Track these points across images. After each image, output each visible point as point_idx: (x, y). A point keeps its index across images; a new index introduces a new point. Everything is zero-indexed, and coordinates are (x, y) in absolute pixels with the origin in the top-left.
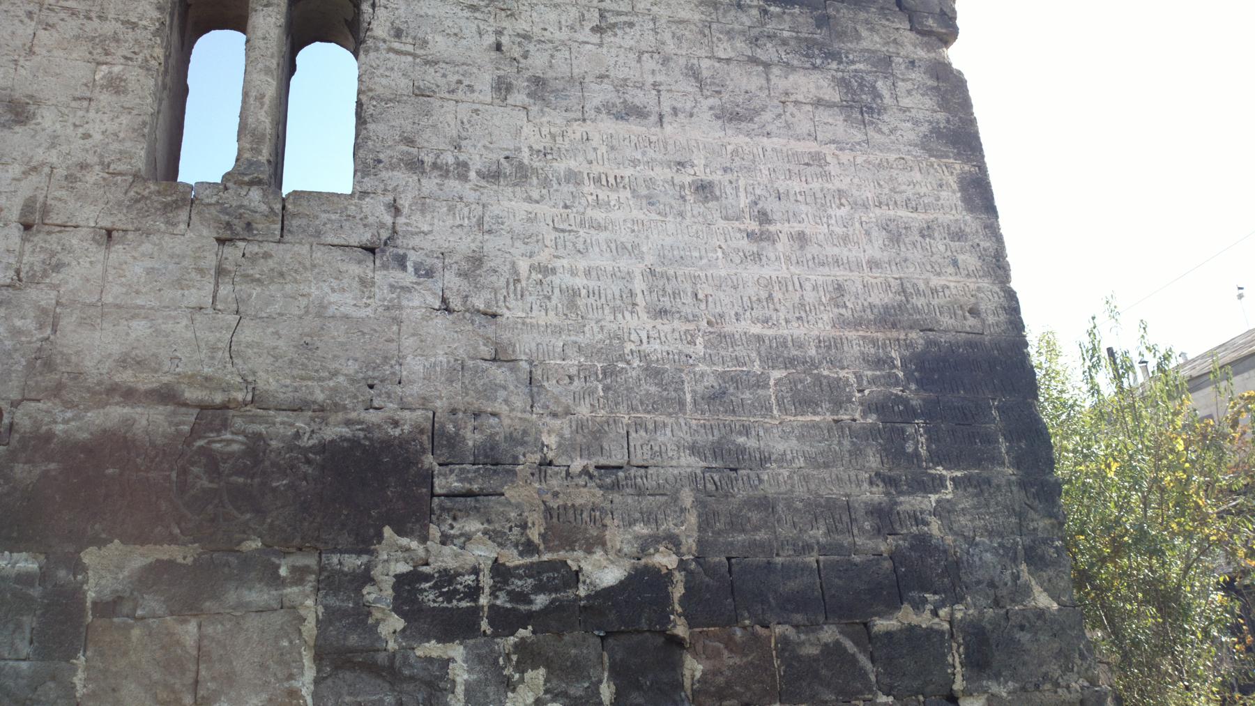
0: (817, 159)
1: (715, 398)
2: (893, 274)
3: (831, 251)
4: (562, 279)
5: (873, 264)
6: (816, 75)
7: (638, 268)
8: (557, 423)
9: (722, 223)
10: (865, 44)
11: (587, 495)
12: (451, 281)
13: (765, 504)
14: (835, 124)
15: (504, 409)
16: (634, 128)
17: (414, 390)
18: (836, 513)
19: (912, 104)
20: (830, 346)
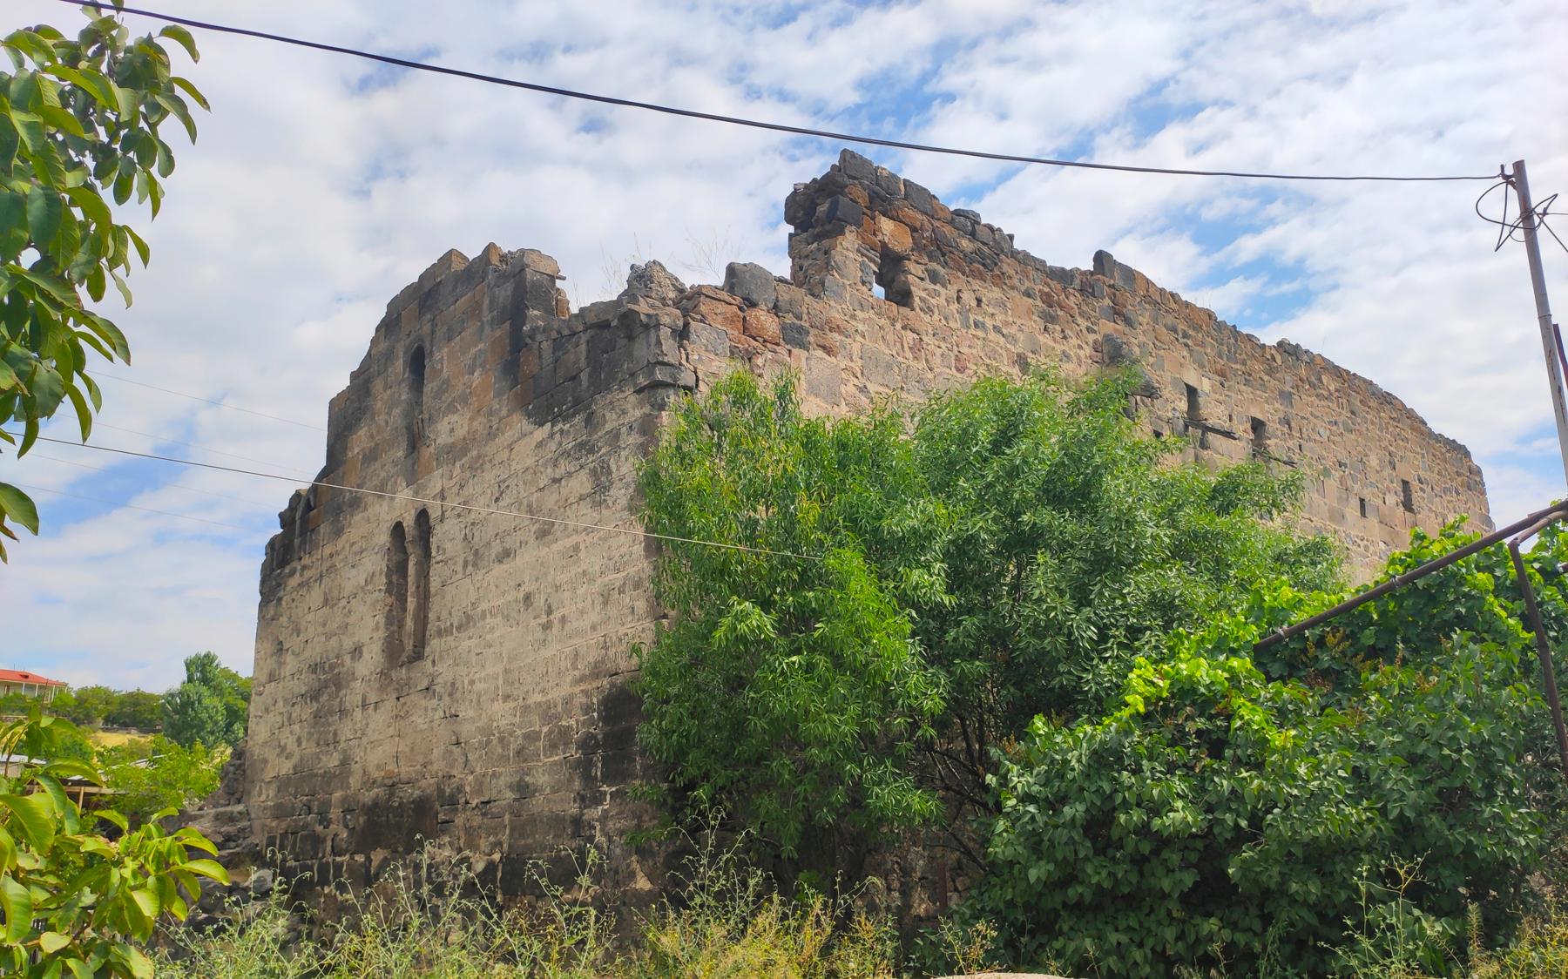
0: (576, 548)
1: (519, 753)
2: (597, 636)
3: (575, 624)
4: (479, 686)
5: (594, 628)
6: (582, 472)
7: (499, 668)
8: (471, 778)
9: (533, 623)
10: (608, 427)
11: (477, 821)
12: (446, 699)
13: (532, 820)
14: (587, 512)
15: (454, 772)
16: (505, 567)
17: (434, 768)
18: (557, 822)
19: (627, 467)
20: (568, 701)
